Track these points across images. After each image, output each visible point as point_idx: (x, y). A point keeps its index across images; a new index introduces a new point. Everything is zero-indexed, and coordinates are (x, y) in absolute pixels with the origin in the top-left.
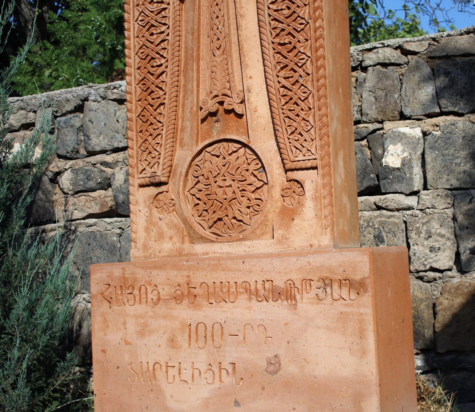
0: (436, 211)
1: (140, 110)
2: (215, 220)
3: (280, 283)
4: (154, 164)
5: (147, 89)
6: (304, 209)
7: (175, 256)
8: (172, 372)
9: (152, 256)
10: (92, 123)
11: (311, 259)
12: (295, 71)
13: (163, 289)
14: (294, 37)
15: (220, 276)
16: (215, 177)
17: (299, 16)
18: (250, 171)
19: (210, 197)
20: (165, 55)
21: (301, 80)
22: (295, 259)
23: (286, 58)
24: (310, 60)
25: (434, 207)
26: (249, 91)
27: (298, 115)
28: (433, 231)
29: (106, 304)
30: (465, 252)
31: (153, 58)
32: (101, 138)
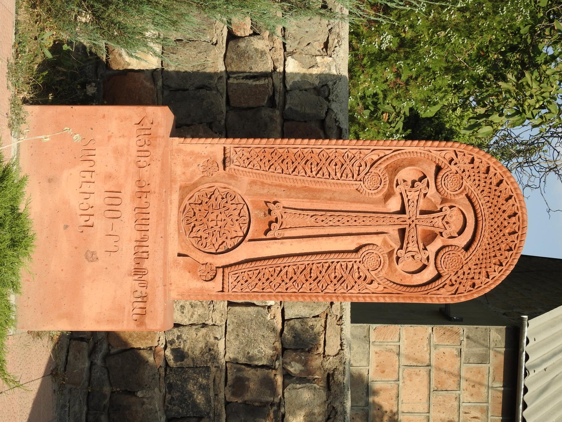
0: (211, 312)
3: (146, 264)
7: (171, 177)
8: (88, 175)
9: (173, 157)
10: (310, 20)
11: (161, 288)
12: (290, 280)
13: (147, 171)
14: (314, 280)
15: (153, 217)
17: (328, 285)
18: (226, 240)
20: (318, 175)
21: (283, 284)
22: (161, 277)
23: (301, 273)
25: (214, 310)
26: (282, 243)
27: (260, 280)
28: (196, 309)
30: (179, 331)
31: (318, 164)
32: (295, 28)
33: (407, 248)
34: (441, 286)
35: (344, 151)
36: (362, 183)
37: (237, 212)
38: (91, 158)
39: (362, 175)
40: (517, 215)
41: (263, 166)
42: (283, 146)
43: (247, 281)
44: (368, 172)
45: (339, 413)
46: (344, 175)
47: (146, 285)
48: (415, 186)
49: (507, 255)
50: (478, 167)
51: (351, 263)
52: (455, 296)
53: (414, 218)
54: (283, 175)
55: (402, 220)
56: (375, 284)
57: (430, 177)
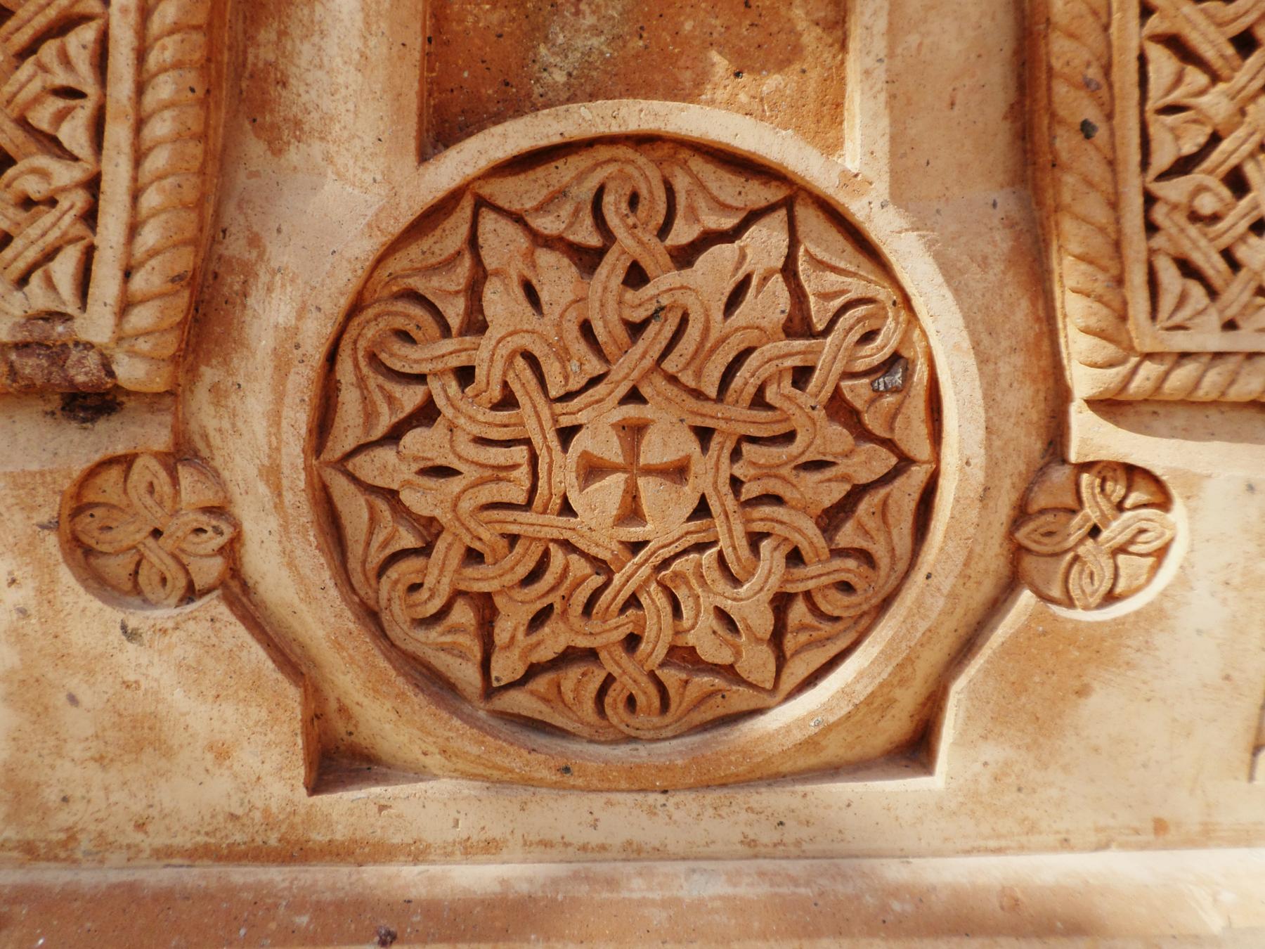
2: (546, 653)
4: (50, 255)
6: (1159, 639)
16: (568, 396)
37: (556, 278)
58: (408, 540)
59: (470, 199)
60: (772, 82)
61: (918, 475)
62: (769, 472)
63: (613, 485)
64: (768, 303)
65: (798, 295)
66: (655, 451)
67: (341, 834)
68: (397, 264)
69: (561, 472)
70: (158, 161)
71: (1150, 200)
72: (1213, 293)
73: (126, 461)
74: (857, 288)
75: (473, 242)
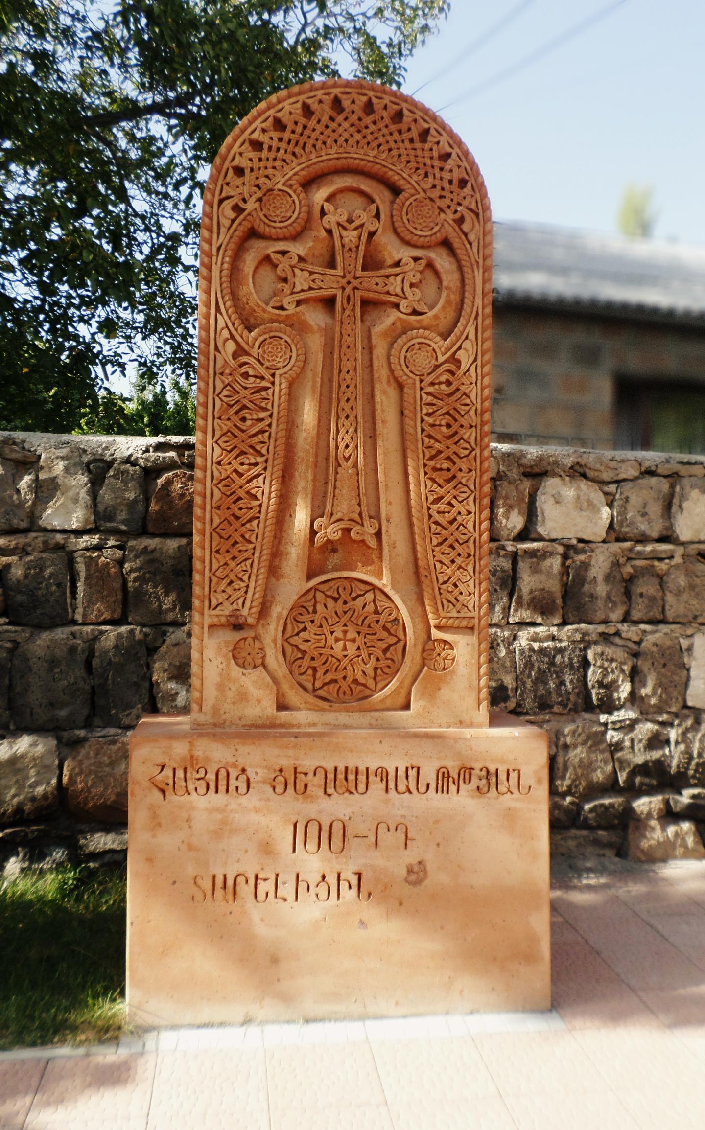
1: (217, 521)
2: (327, 680)
5: (232, 494)
8: (263, 887)
12: (454, 507)
13: (256, 773)
14: (454, 463)
17: (462, 438)
19: (323, 651)
20: (264, 451)
24: (473, 495)
29: (158, 795)
33: (396, 295)
34: (463, 237)
35: (218, 403)
36: (278, 372)
37: (330, 603)
38: (230, 883)
39: (262, 371)
40: (339, 95)
41: (246, 555)
42: (208, 516)
43: (456, 586)
44: (259, 360)
45: (579, 460)
46: (263, 405)
47: (467, 771)
48: (284, 275)
49: (410, 119)
50: (251, 160)
51: (424, 396)
52: (481, 212)
53: (344, 281)
54: (263, 516)
55: (345, 302)
56: (461, 355)
57: (267, 248)
58: (300, 655)
59: (315, 589)
60: (369, 568)
61: (402, 643)
62: (372, 641)
63: (341, 643)
64: (370, 608)
65: (376, 607)
66: (350, 636)
67: (283, 721)
68: (300, 601)
69: (331, 640)
70: (260, 582)
71: (439, 589)
72: (454, 606)
73: (245, 639)
74: (387, 605)
75: (314, 597)
